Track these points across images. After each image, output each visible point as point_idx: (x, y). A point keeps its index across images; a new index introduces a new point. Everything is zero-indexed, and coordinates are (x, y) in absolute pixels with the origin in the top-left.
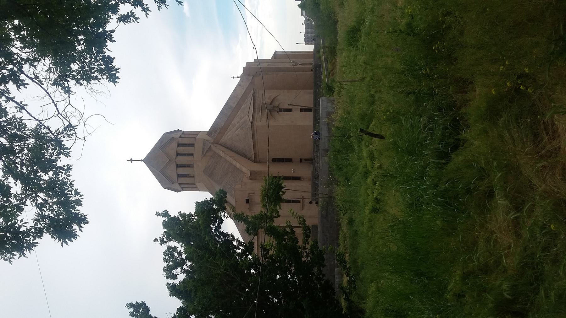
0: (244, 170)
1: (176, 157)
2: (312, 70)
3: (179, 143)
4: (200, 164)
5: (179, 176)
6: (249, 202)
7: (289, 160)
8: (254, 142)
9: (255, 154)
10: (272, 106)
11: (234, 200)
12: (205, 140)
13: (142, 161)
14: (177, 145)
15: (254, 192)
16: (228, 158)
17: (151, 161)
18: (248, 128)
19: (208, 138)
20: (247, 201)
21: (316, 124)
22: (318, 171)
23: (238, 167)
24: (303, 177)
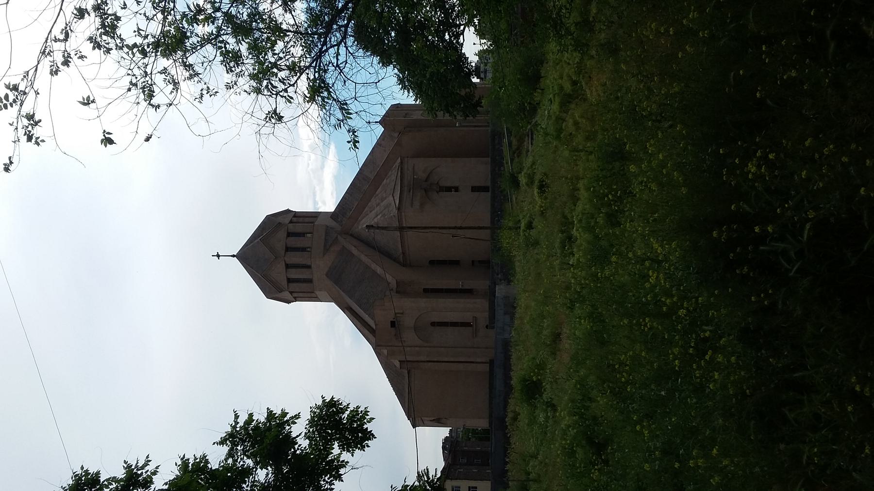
0: (389, 278)
1: (285, 253)
3: (289, 231)
4: (321, 265)
5: (290, 281)
6: (396, 326)
9: (403, 253)
11: (373, 322)
12: (327, 226)
13: (233, 256)
14: (286, 236)
16: (363, 258)
18: (393, 217)
19: (332, 223)
20: (393, 324)
21: (495, 219)
23: (378, 272)
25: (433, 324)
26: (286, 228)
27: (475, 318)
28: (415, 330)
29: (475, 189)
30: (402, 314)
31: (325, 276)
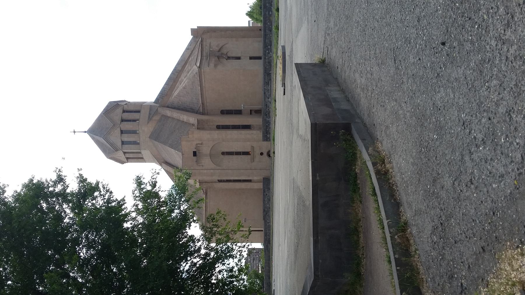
2: (260, 30)
3: (124, 109)
5: (123, 143)
7: (239, 112)
8: (201, 90)
9: (203, 104)
10: (220, 53)
12: (151, 105)
13: (85, 132)
14: (122, 111)
15: (202, 143)
17: (95, 132)
20: (195, 154)
21: (266, 52)
22: (269, 107)
23: (185, 120)
24: (253, 125)
25: (223, 153)
26: (122, 107)
27: (253, 147)
28: (210, 157)
29: (251, 58)
30: (202, 144)
31: (149, 139)
